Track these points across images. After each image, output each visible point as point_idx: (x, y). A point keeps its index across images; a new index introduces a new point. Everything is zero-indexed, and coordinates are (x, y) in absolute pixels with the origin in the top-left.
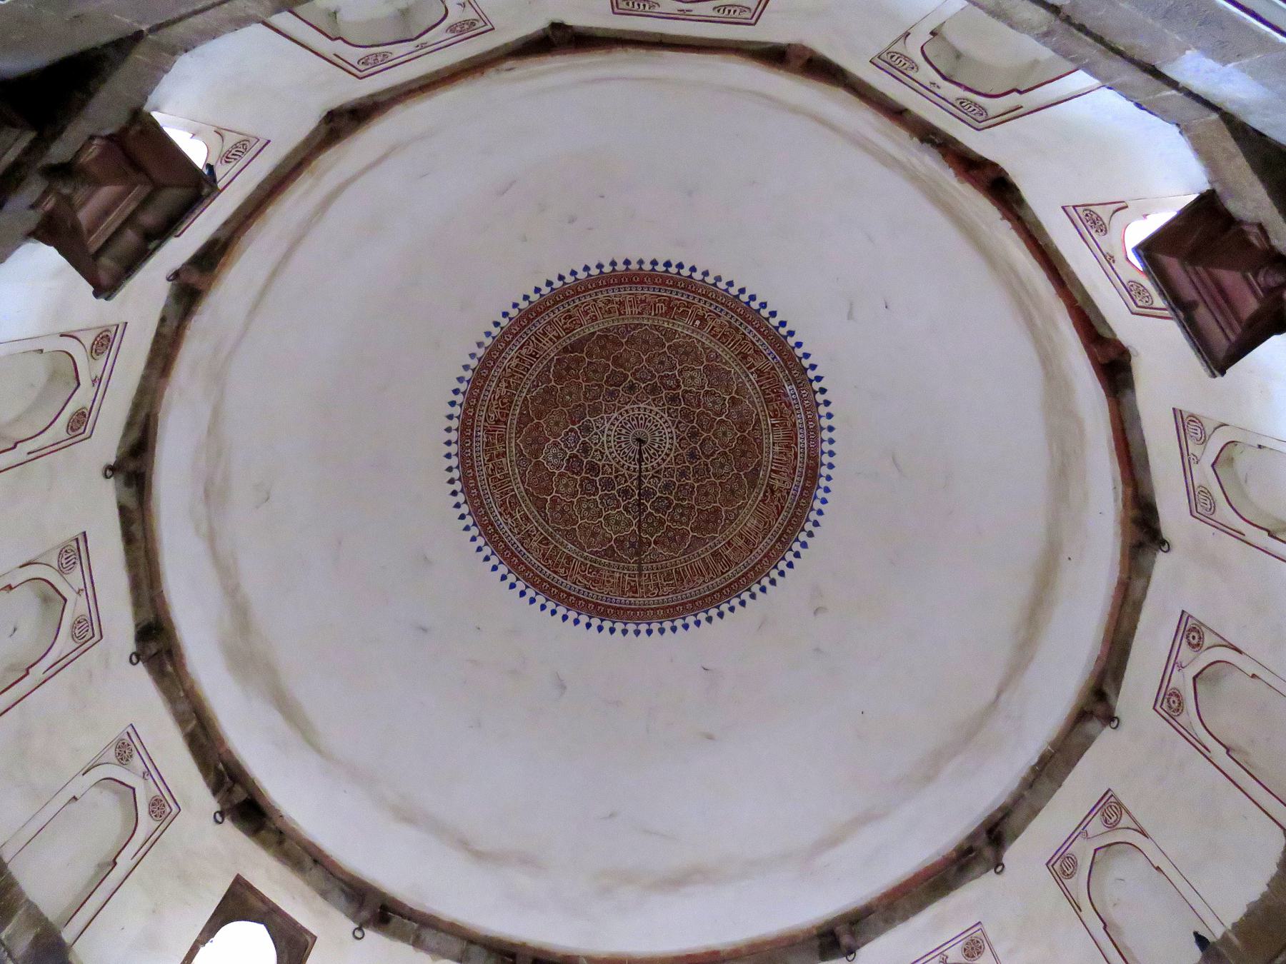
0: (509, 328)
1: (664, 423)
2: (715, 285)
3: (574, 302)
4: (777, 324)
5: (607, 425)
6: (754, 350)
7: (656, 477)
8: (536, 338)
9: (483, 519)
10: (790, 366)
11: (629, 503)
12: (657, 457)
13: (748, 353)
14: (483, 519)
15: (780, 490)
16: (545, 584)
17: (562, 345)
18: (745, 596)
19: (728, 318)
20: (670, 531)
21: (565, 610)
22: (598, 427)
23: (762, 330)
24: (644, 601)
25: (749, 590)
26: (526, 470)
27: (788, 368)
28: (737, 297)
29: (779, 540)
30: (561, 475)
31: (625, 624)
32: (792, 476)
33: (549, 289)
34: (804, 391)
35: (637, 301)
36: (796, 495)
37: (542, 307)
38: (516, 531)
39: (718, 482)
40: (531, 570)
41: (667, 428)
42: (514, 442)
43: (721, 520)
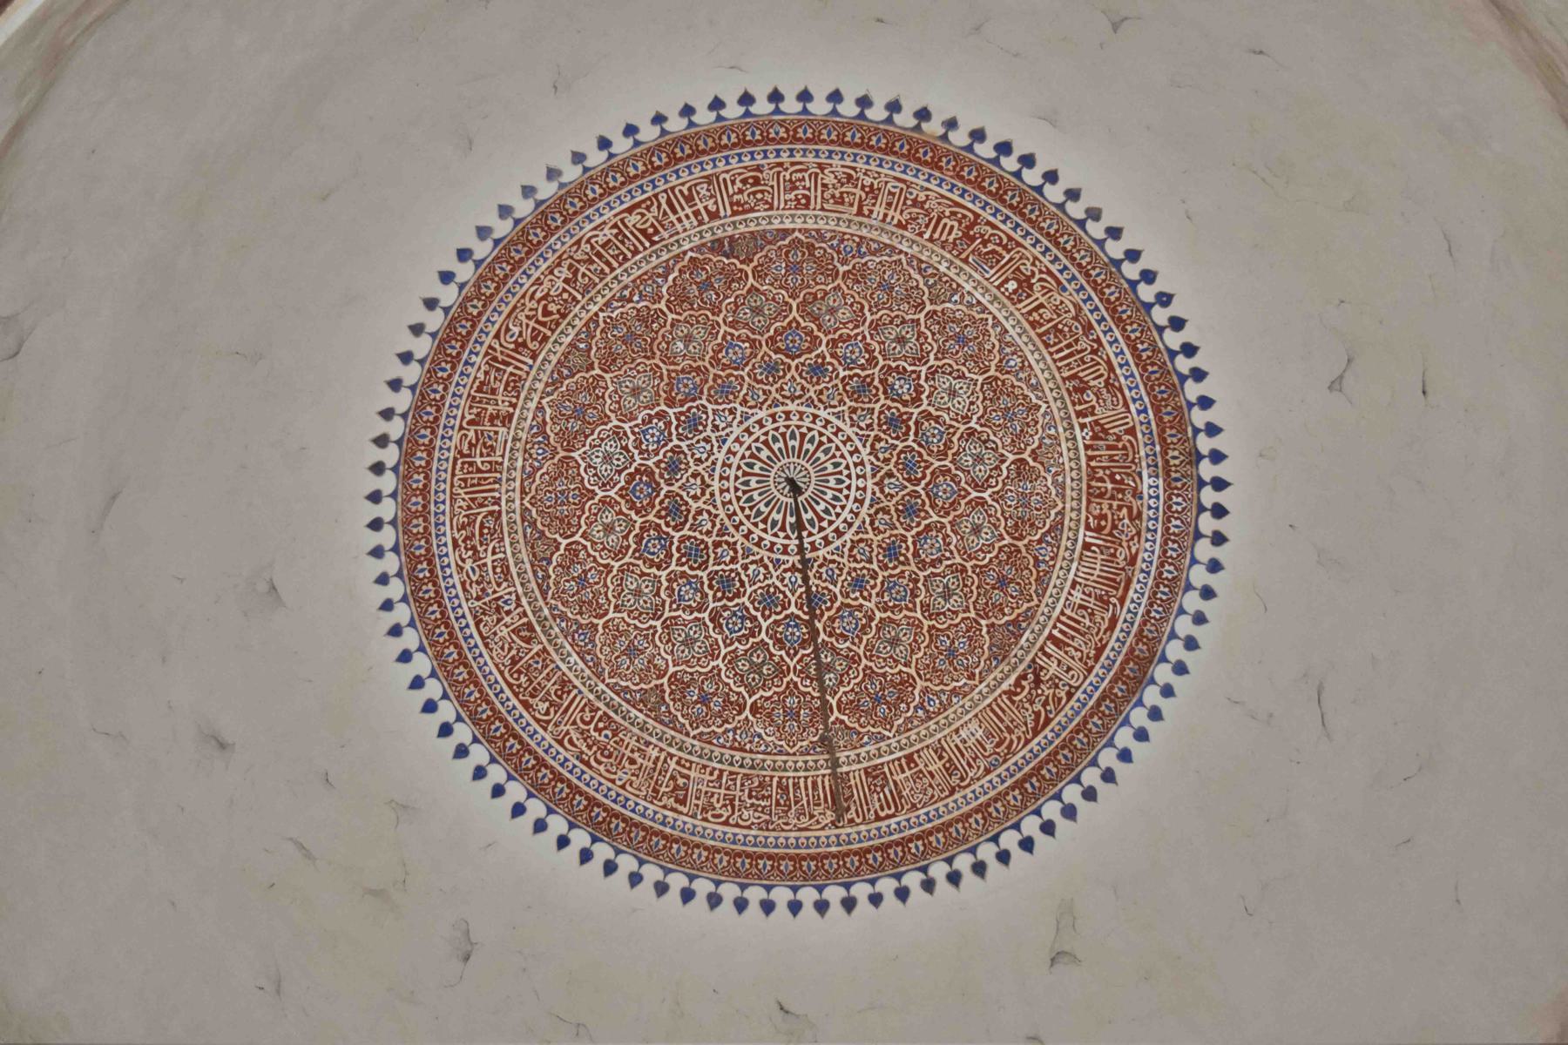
1: (856, 465)
2: (1081, 224)
4: (1176, 347)
5: (737, 431)
6: (1107, 382)
9: (417, 543)
12: (815, 531)
13: (1092, 383)
14: (417, 543)
16: (497, 723)
17: (713, 234)
18: (913, 880)
19: (1078, 298)
21: (525, 794)
22: (716, 428)
23: (1140, 346)
24: (695, 826)
25: (924, 870)
26: (539, 469)
27: (1163, 440)
28: (1117, 263)
29: (1019, 785)
31: (641, 862)
32: (1090, 663)
33: (742, 110)
34: (1180, 500)
36: (1084, 705)
37: (709, 140)
38: (474, 591)
39: (926, 623)
40: (476, 684)
41: (858, 477)
42: (536, 399)
43: (908, 704)
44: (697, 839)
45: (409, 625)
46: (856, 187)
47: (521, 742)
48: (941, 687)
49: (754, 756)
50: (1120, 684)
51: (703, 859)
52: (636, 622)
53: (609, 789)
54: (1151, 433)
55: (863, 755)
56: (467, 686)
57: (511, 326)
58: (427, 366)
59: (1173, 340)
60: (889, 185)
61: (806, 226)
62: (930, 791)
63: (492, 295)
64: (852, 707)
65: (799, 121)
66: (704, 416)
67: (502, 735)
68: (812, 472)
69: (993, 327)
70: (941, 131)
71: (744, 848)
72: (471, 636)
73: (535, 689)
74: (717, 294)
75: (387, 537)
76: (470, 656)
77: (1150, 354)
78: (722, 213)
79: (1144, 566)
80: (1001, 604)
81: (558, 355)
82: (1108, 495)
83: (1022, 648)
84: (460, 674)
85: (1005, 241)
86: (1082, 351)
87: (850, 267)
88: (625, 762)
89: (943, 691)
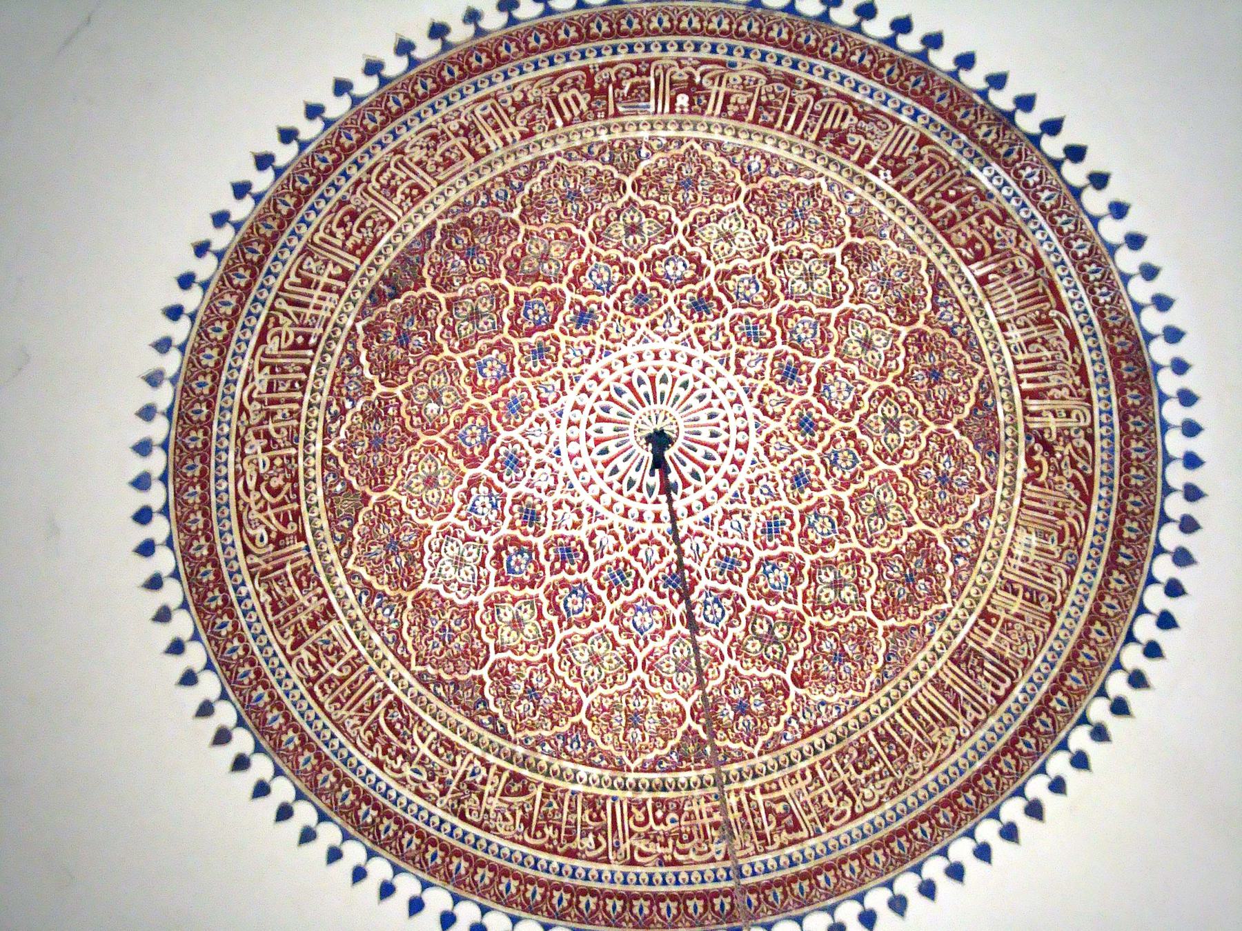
3: (348, 178)
4: (887, 32)
6: (856, 113)
7: (736, 512)
8: (291, 302)
9: (339, 795)
10: (967, 122)
12: (718, 461)
13: (845, 126)
14: (339, 795)
16: (556, 894)
18: (1080, 739)
19: (754, 61)
20: (823, 638)
22: (539, 447)
24: (826, 844)
25: (1084, 720)
26: (400, 628)
27: (961, 127)
29: (1112, 565)
34: (1029, 170)
35: (506, 111)
36: (1112, 438)
37: (270, 222)
38: (433, 789)
39: (896, 468)
40: (506, 873)
42: (340, 570)
43: (943, 562)
44: (837, 854)
45: (395, 874)
46: (449, 139)
47: (593, 893)
48: (961, 520)
49: (832, 728)
50: (1129, 392)
51: (857, 870)
52: (616, 687)
53: (715, 871)
54: (943, 128)
55: (938, 646)
57: (251, 532)
58: (204, 637)
60: (478, 112)
61: (439, 211)
62: (1031, 636)
63: (206, 524)
64: (890, 606)
66: (517, 447)
67: (570, 903)
68: (668, 408)
69: (704, 149)
70: (470, 29)
71: (890, 828)
72: (465, 833)
73: (567, 831)
74: (423, 335)
75: (305, 814)
76: (479, 853)
77: (871, 57)
78: (352, 267)
79: (1053, 259)
80: (951, 397)
81: (324, 515)
82: (959, 217)
83: (1006, 425)
84: (483, 878)
85: (634, 69)
86: (806, 106)
87: (520, 207)
89: (966, 524)
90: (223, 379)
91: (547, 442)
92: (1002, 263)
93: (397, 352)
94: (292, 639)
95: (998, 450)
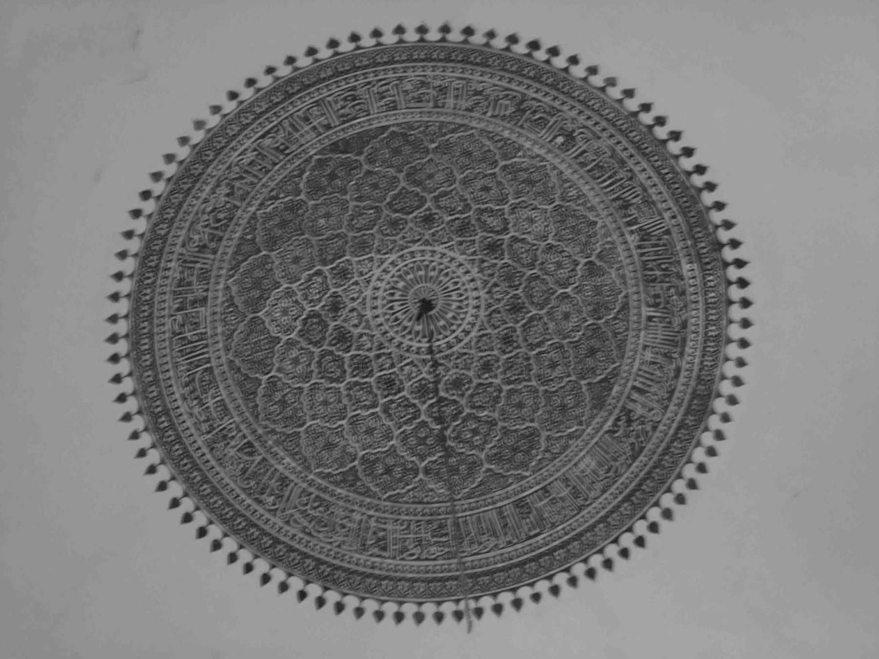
0: (251, 105)
2: (603, 89)
5: (377, 272)
8: (292, 126)
11: (392, 401)
15: (642, 420)
18: (561, 579)
26: (234, 330)
28: (635, 114)
29: (627, 499)
30: (291, 344)
32: (666, 402)
36: (666, 435)
38: (205, 427)
52: (327, 424)
56: (212, 498)
57: (191, 236)
58: (135, 279)
59: (687, 164)
63: (173, 218)
65: (375, 51)
66: (350, 267)
70: (484, 41)
75: (132, 405)
76: (209, 475)
77: (670, 175)
78: (332, 125)
83: (614, 398)
86: (622, 179)
88: (338, 529)
90: (231, 146)
91: (366, 274)
92: (665, 315)
93: (324, 181)
94: (177, 306)
95: (601, 409)
